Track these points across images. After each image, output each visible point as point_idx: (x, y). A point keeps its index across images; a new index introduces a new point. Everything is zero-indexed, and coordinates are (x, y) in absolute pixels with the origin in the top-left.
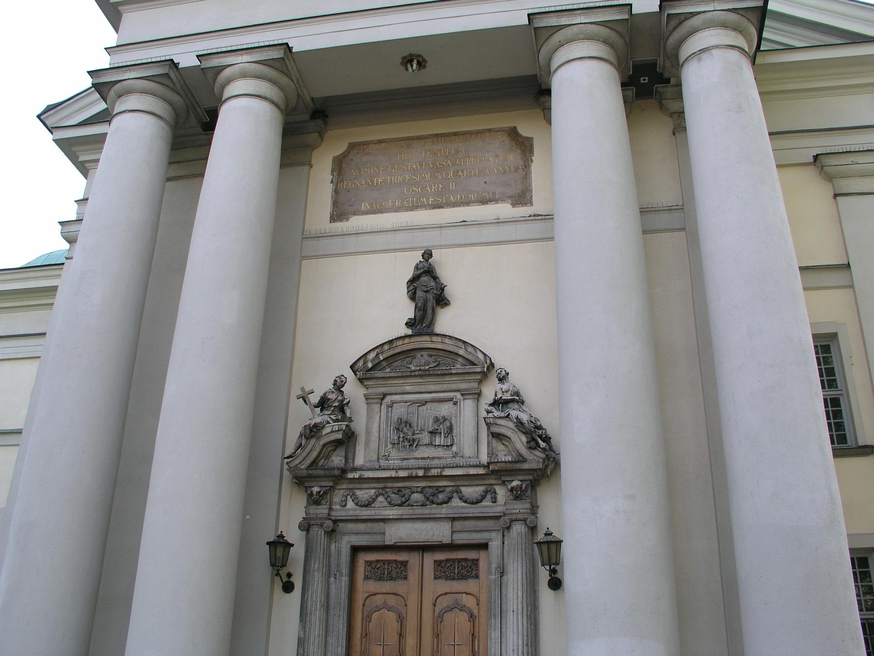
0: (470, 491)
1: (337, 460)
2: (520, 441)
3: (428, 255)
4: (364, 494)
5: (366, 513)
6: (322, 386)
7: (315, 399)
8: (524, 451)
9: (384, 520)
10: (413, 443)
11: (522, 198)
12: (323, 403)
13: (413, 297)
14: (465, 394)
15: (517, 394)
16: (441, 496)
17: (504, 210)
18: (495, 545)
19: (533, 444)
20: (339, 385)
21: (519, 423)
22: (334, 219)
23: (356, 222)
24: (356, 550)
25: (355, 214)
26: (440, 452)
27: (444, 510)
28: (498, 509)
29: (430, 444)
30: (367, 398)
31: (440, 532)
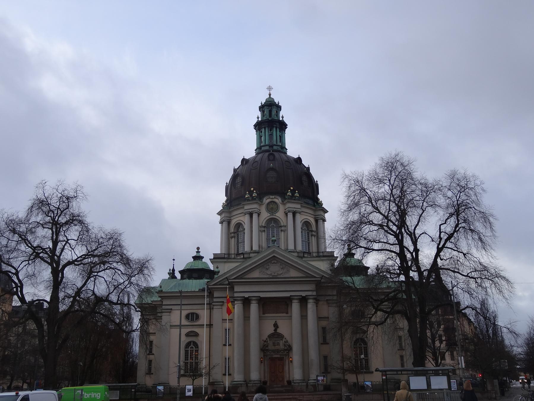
0: (282, 352)
1: (267, 348)
2: (288, 347)
3: (276, 321)
4: (270, 352)
5: (271, 354)
6: (265, 339)
7: (264, 340)
8: (288, 348)
9: (273, 355)
10: (275, 346)
11: (287, 313)
12: (265, 341)
13: (274, 327)
14: (281, 340)
15: (287, 341)
16: (279, 352)
17: (285, 315)
18: (285, 358)
19: (289, 347)
20: (267, 339)
21: (288, 345)
22: (263, 314)
23: (266, 315)
24: (269, 358)
25: (266, 314)
26: (278, 347)
27: (279, 354)
28: (285, 354)
29: (277, 346)
30: (270, 340)
31: (279, 356)
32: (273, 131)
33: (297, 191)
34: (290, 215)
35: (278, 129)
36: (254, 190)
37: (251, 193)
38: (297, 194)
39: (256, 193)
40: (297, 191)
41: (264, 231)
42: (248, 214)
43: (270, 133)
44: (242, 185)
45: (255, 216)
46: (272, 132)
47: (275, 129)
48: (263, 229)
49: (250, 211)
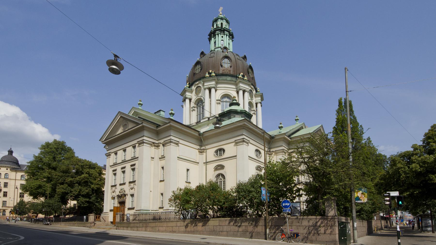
32: (224, 38)
33: (246, 76)
34: (241, 92)
35: (228, 36)
36: (212, 72)
37: (209, 73)
38: (246, 78)
39: (214, 73)
40: (246, 76)
41: (220, 103)
42: (207, 89)
43: (222, 39)
44: (201, 70)
45: (213, 90)
46: (223, 38)
47: (225, 36)
48: (219, 102)
49: (209, 86)
